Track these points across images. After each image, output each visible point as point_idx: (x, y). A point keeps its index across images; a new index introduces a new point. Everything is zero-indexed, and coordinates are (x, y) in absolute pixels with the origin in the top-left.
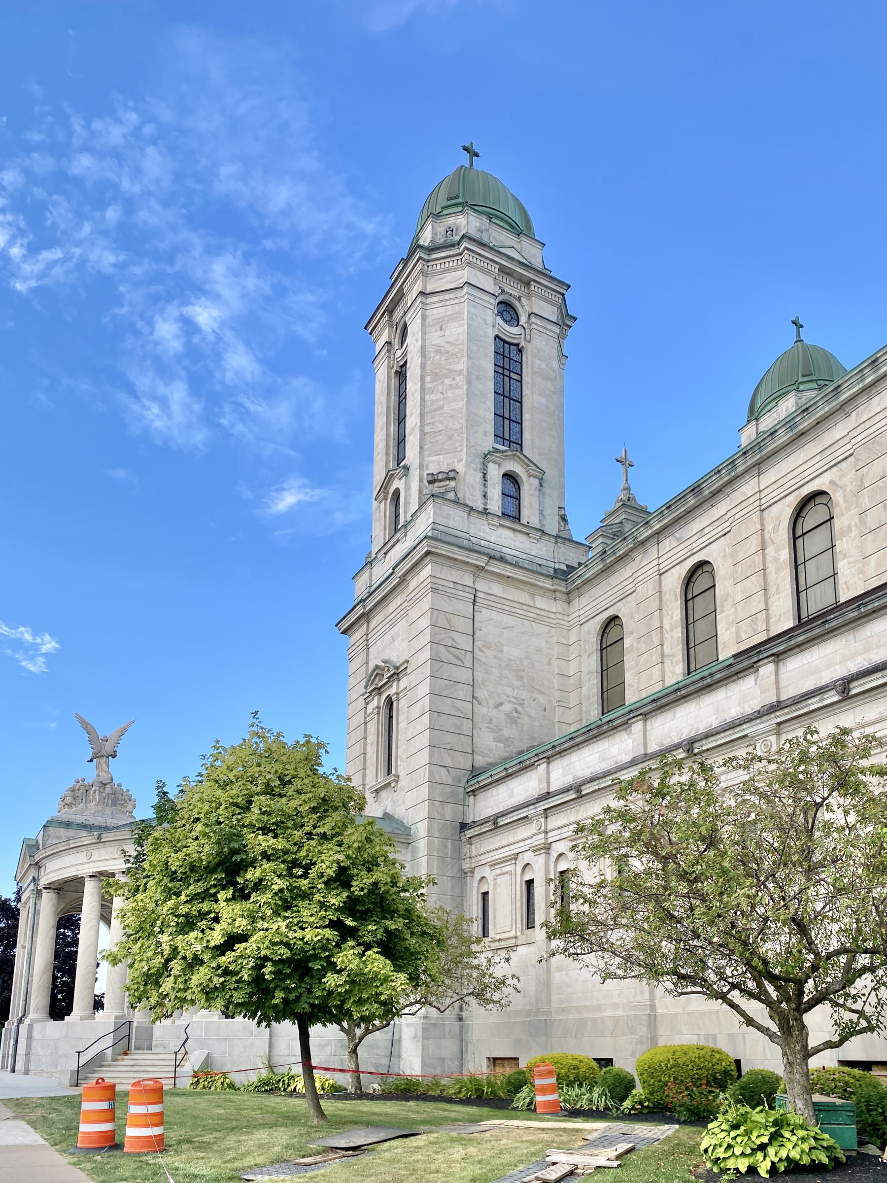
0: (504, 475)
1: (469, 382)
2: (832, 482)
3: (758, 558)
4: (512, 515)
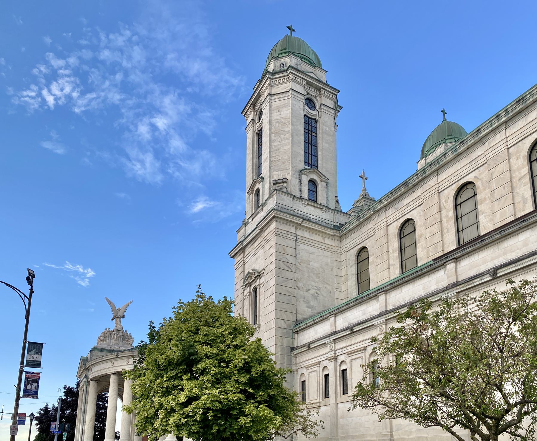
0: (309, 181)
1: (292, 136)
2: (476, 177)
3: (437, 216)
4: (313, 199)
